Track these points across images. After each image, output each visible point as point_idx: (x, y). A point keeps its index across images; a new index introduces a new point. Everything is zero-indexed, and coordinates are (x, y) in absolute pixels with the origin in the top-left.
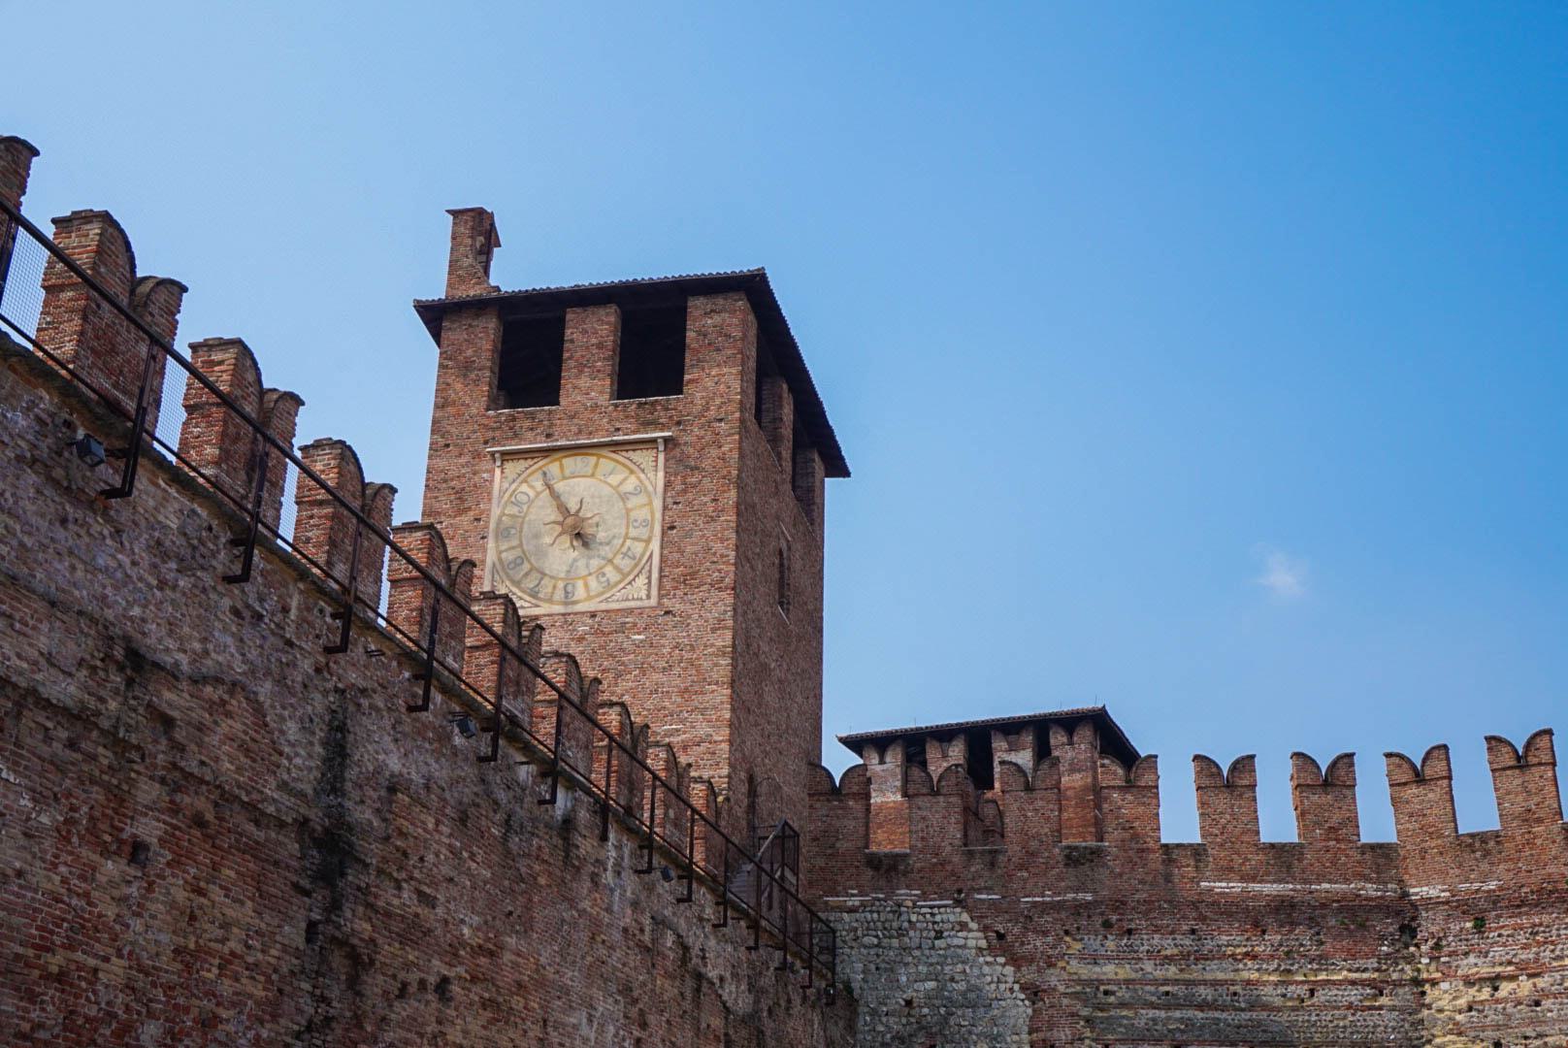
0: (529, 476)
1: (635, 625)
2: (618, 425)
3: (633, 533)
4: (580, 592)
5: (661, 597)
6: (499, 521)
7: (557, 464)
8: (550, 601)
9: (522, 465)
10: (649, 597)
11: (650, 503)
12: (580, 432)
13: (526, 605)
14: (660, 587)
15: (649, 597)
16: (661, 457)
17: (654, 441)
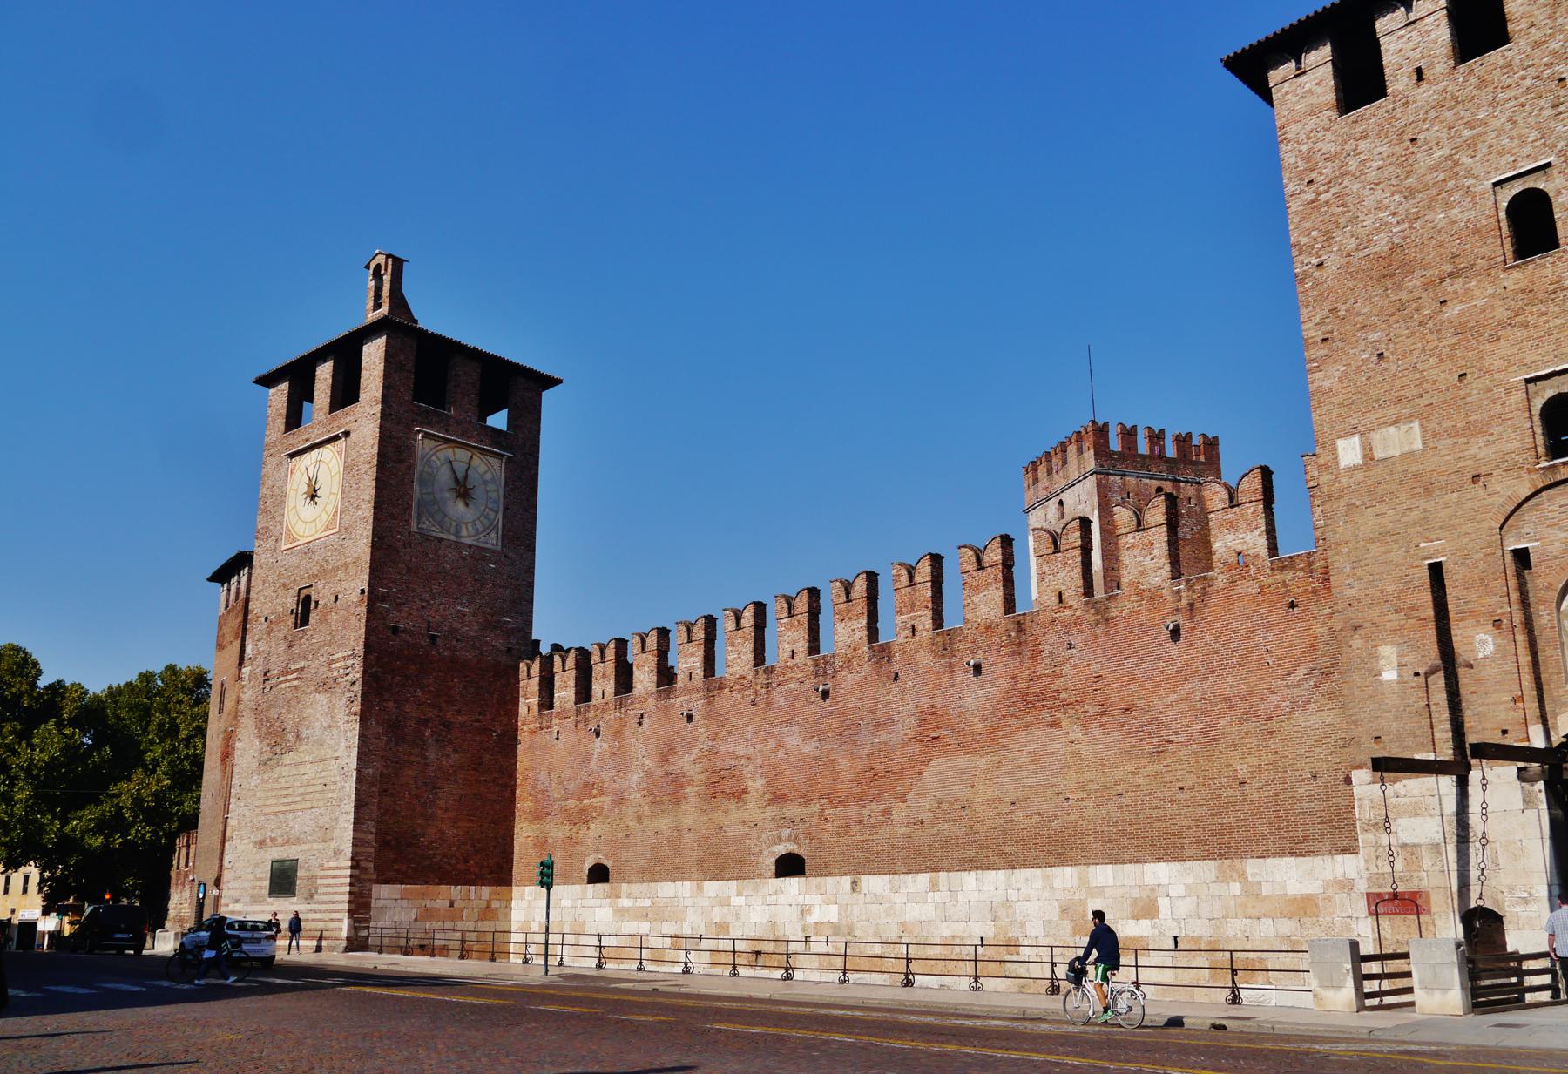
0: (437, 451)
1: (490, 558)
2: (482, 438)
3: (490, 505)
4: (464, 532)
5: (502, 546)
6: (421, 475)
7: (451, 450)
8: (448, 531)
9: (433, 443)
10: (497, 545)
11: (498, 491)
12: (463, 434)
13: (436, 530)
14: (502, 541)
15: (497, 545)
16: (503, 466)
17: (503, 455)
